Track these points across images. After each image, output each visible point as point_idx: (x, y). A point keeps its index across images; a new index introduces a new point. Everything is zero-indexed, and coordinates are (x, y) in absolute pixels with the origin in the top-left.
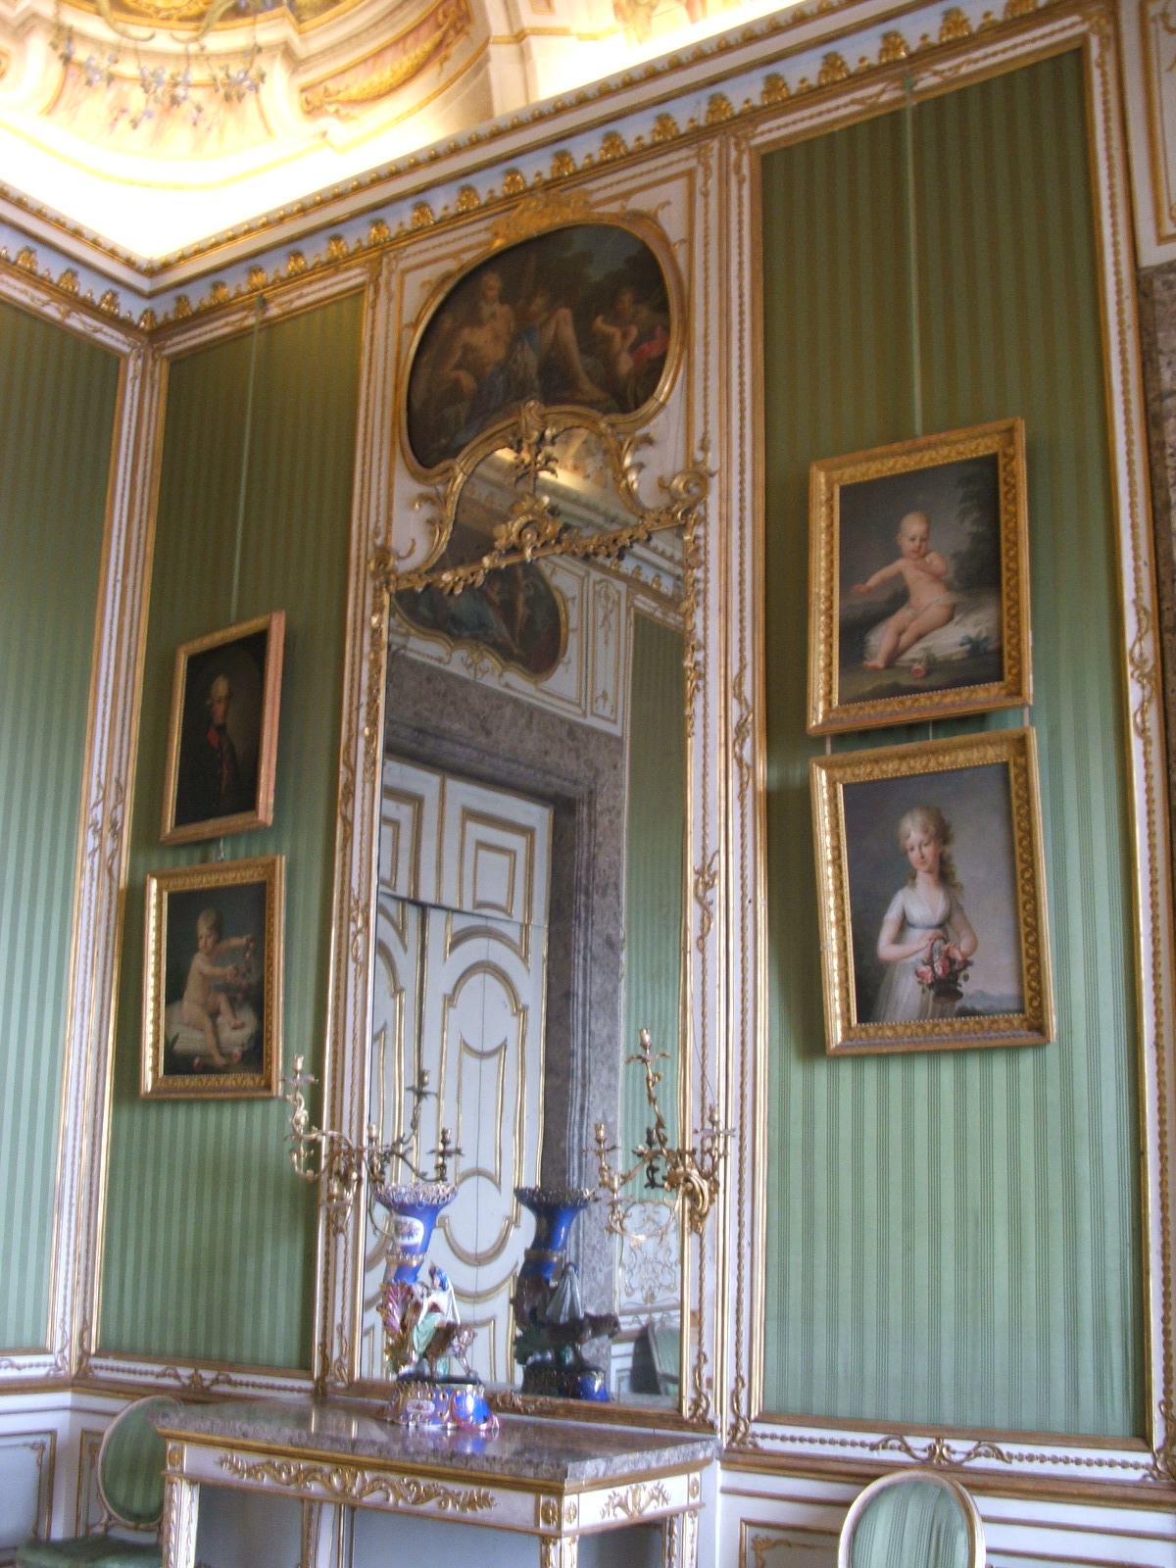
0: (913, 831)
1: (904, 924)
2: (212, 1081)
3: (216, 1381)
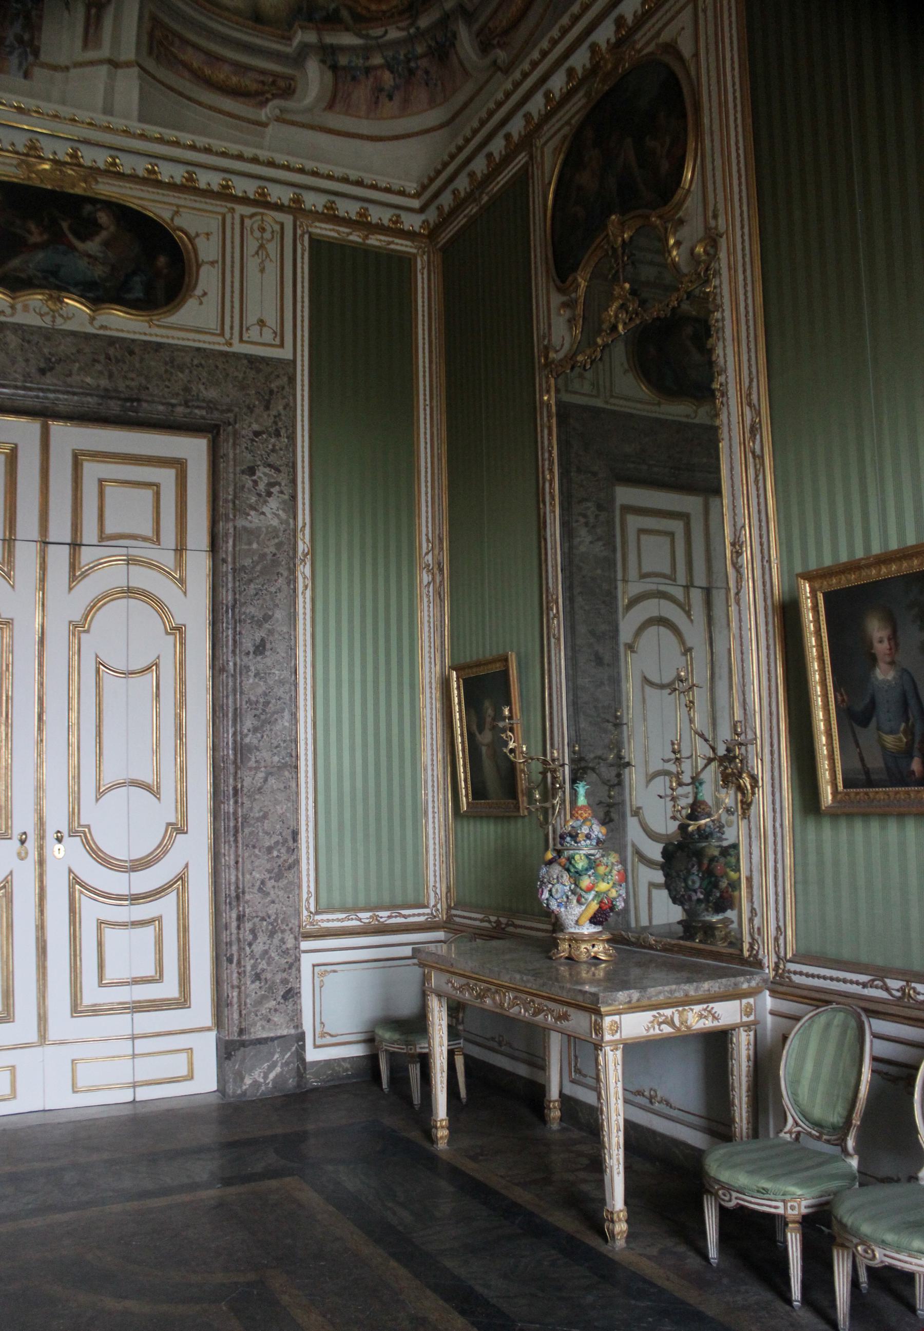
3: (507, 925)
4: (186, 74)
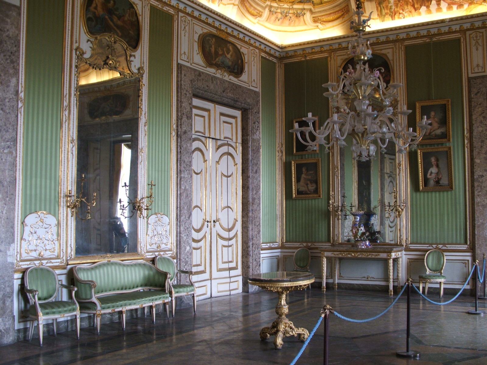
0: (433, 160)
1: (431, 173)
2: (308, 196)
3: (311, 245)
4: (245, 9)
